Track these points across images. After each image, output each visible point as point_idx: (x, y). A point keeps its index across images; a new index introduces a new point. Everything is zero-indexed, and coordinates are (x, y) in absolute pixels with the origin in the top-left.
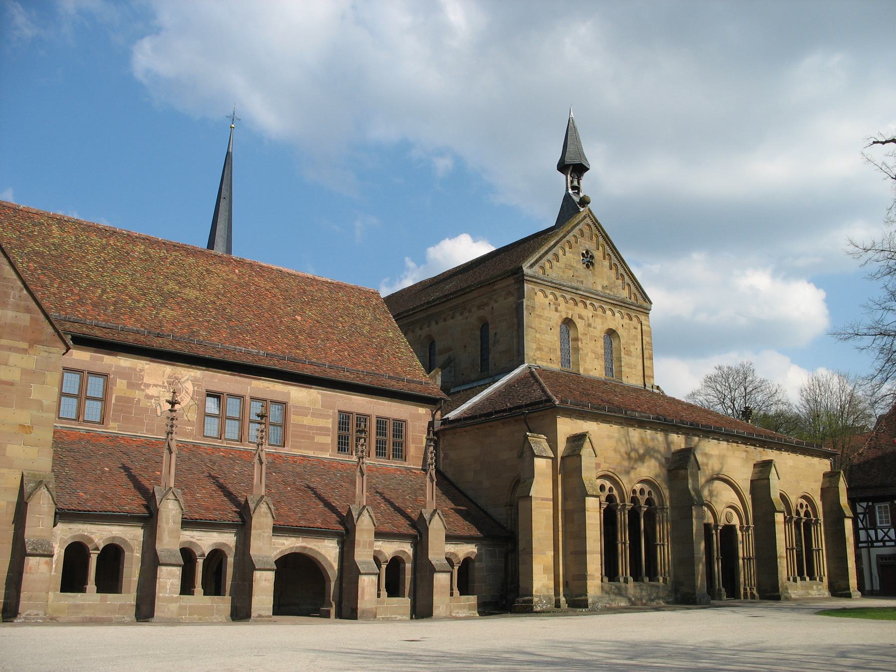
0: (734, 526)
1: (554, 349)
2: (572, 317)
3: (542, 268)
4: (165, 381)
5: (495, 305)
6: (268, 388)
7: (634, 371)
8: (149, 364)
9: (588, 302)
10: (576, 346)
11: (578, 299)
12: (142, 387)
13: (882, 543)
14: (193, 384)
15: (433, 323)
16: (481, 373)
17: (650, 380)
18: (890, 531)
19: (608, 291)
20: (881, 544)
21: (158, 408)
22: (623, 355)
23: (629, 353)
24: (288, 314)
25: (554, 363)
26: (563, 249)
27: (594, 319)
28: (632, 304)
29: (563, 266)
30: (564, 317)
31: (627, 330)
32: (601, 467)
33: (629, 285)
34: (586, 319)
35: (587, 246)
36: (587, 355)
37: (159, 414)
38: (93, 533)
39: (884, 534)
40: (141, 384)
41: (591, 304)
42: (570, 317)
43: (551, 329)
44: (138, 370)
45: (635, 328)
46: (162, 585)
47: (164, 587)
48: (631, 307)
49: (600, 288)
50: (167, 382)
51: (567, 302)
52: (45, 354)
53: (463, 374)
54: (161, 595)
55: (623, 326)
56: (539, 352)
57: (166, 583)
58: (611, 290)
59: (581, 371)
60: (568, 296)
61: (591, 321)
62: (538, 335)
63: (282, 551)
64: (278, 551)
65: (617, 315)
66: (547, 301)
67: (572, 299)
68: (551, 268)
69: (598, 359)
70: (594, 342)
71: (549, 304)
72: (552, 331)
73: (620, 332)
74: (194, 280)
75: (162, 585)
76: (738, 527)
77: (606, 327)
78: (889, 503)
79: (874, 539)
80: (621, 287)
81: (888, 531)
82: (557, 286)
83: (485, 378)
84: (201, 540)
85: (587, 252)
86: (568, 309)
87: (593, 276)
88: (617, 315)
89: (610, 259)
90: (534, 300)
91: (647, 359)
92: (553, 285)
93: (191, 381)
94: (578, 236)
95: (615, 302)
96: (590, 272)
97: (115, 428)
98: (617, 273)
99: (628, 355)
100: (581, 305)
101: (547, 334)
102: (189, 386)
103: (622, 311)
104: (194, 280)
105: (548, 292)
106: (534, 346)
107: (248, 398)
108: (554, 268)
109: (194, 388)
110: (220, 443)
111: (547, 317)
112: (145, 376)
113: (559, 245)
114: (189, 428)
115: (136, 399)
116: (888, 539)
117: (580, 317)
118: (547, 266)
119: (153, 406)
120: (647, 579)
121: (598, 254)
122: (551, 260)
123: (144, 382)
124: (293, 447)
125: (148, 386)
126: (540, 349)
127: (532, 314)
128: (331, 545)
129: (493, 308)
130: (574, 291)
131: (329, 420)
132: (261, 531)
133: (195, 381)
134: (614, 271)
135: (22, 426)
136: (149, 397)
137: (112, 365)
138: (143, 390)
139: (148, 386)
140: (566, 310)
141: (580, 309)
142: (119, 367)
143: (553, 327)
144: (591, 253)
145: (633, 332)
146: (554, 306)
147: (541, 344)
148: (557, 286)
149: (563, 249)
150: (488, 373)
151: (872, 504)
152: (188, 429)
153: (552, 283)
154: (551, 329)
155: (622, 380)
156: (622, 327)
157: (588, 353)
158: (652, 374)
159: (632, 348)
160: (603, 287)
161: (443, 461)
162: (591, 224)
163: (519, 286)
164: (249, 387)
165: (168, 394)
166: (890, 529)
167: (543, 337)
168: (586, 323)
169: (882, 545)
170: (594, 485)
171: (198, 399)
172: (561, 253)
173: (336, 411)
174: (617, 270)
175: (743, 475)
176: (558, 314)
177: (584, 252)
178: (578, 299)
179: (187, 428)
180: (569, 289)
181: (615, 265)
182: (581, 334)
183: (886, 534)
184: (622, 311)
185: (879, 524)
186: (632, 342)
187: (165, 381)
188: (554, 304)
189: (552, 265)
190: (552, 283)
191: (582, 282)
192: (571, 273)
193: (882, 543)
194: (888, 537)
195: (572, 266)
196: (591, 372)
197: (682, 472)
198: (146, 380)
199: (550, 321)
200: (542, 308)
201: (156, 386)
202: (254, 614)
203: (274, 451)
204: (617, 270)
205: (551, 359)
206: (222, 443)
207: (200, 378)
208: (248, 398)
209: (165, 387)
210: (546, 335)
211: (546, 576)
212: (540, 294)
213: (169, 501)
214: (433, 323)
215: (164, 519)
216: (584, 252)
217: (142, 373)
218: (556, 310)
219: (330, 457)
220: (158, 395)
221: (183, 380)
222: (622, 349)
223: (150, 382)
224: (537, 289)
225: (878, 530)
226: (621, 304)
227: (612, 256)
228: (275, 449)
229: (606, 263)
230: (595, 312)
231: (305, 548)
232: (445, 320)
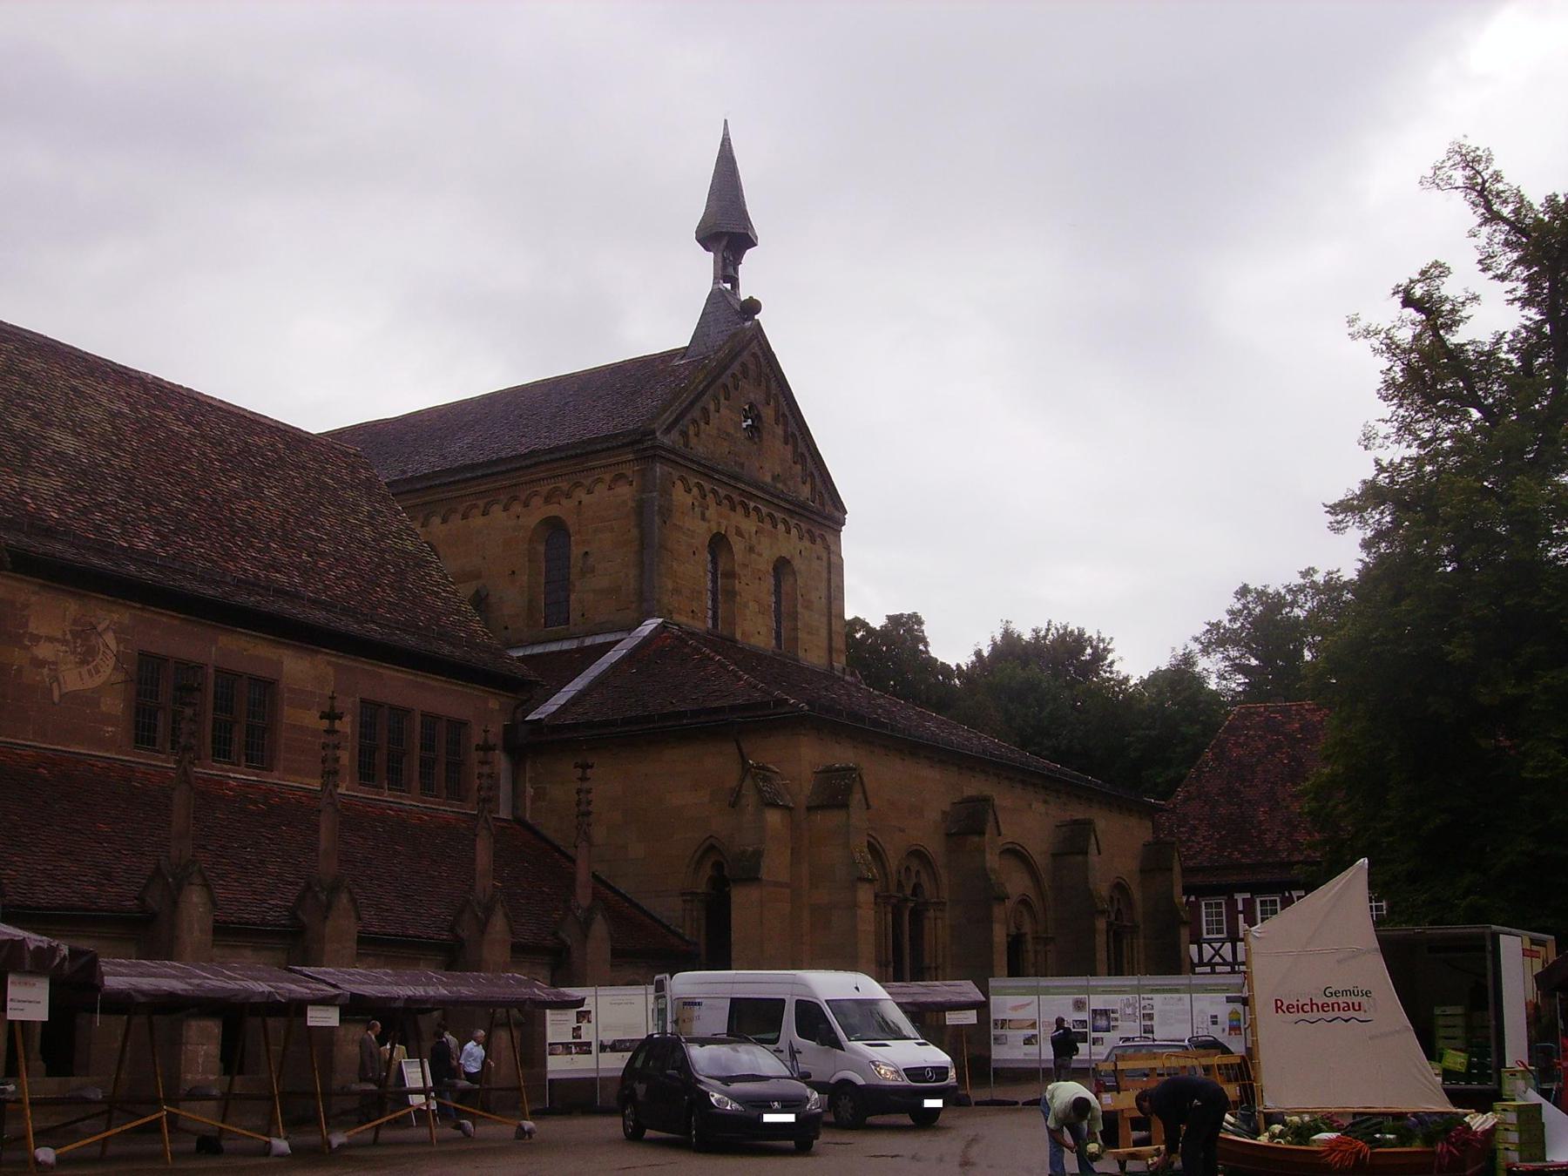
0: (1026, 934)
2: (726, 532)
3: (684, 434)
5: (586, 498)
6: (245, 650)
9: (752, 505)
11: (737, 498)
13: (1229, 967)
14: (116, 638)
15: (437, 520)
16: (545, 627)
18: (1224, 947)
19: (780, 486)
20: (1208, 969)
21: (55, 684)
22: (800, 609)
23: (808, 605)
25: (698, 619)
26: (716, 398)
34: (747, 536)
35: (752, 396)
37: (56, 699)
39: (1213, 952)
41: (756, 509)
43: (694, 553)
45: (818, 558)
48: (815, 517)
49: (768, 479)
51: (719, 504)
53: (506, 628)
59: (738, 636)
60: (722, 492)
65: (794, 531)
66: (689, 500)
67: (728, 497)
68: (697, 435)
70: (757, 581)
71: (693, 504)
73: (797, 563)
74: (59, 411)
76: (1029, 937)
78: (1226, 898)
79: (1196, 960)
81: (1221, 947)
82: (707, 470)
83: (562, 639)
85: (751, 406)
88: (794, 531)
89: (786, 424)
90: (671, 495)
92: (701, 469)
93: (115, 632)
94: (740, 376)
95: (791, 507)
96: (755, 446)
100: (739, 509)
104: (59, 411)
105: (693, 480)
106: (670, 585)
108: (703, 435)
114: (110, 729)
115: (15, 667)
116: (1221, 961)
117: (739, 533)
118: (691, 432)
119: (45, 682)
121: (768, 413)
122: (698, 419)
123: (30, 630)
125: (36, 639)
127: (668, 522)
129: (580, 502)
134: (789, 447)
136: (39, 663)
139: (36, 639)
140: (719, 518)
141: (738, 518)
144: (759, 411)
146: (700, 509)
147: (678, 581)
148: (707, 470)
149: (716, 398)
150: (568, 629)
151: (1196, 899)
152: (108, 732)
153: (699, 464)
154: (694, 553)
161: (533, 802)
162: (760, 354)
163: (643, 467)
165: (72, 658)
166: (1224, 943)
169: (1230, 970)
172: (712, 407)
173: (358, 700)
175: (1040, 845)
176: (705, 525)
177: (747, 407)
178: (737, 498)
179: (105, 728)
180: (725, 479)
181: (793, 435)
182: (739, 565)
183: (1217, 952)
184: (802, 525)
185: (1205, 936)
188: (700, 506)
189: (698, 430)
190: (699, 464)
191: (742, 465)
193: (1229, 967)
194: (1221, 956)
195: (728, 434)
197: (976, 839)
198: (33, 627)
200: (683, 513)
201: (50, 639)
203: (255, 778)
204: (795, 446)
205: (693, 611)
212: (679, 483)
213: (193, 887)
214: (437, 520)
216: (747, 407)
218: (703, 518)
219: (347, 793)
220: (54, 659)
222: (799, 597)
223: (43, 631)
224: (676, 474)
225: (1204, 945)
226: (801, 511)
228: (257, 776)
229: (779, 431)
230: (760, 524)
232: (465, 517)
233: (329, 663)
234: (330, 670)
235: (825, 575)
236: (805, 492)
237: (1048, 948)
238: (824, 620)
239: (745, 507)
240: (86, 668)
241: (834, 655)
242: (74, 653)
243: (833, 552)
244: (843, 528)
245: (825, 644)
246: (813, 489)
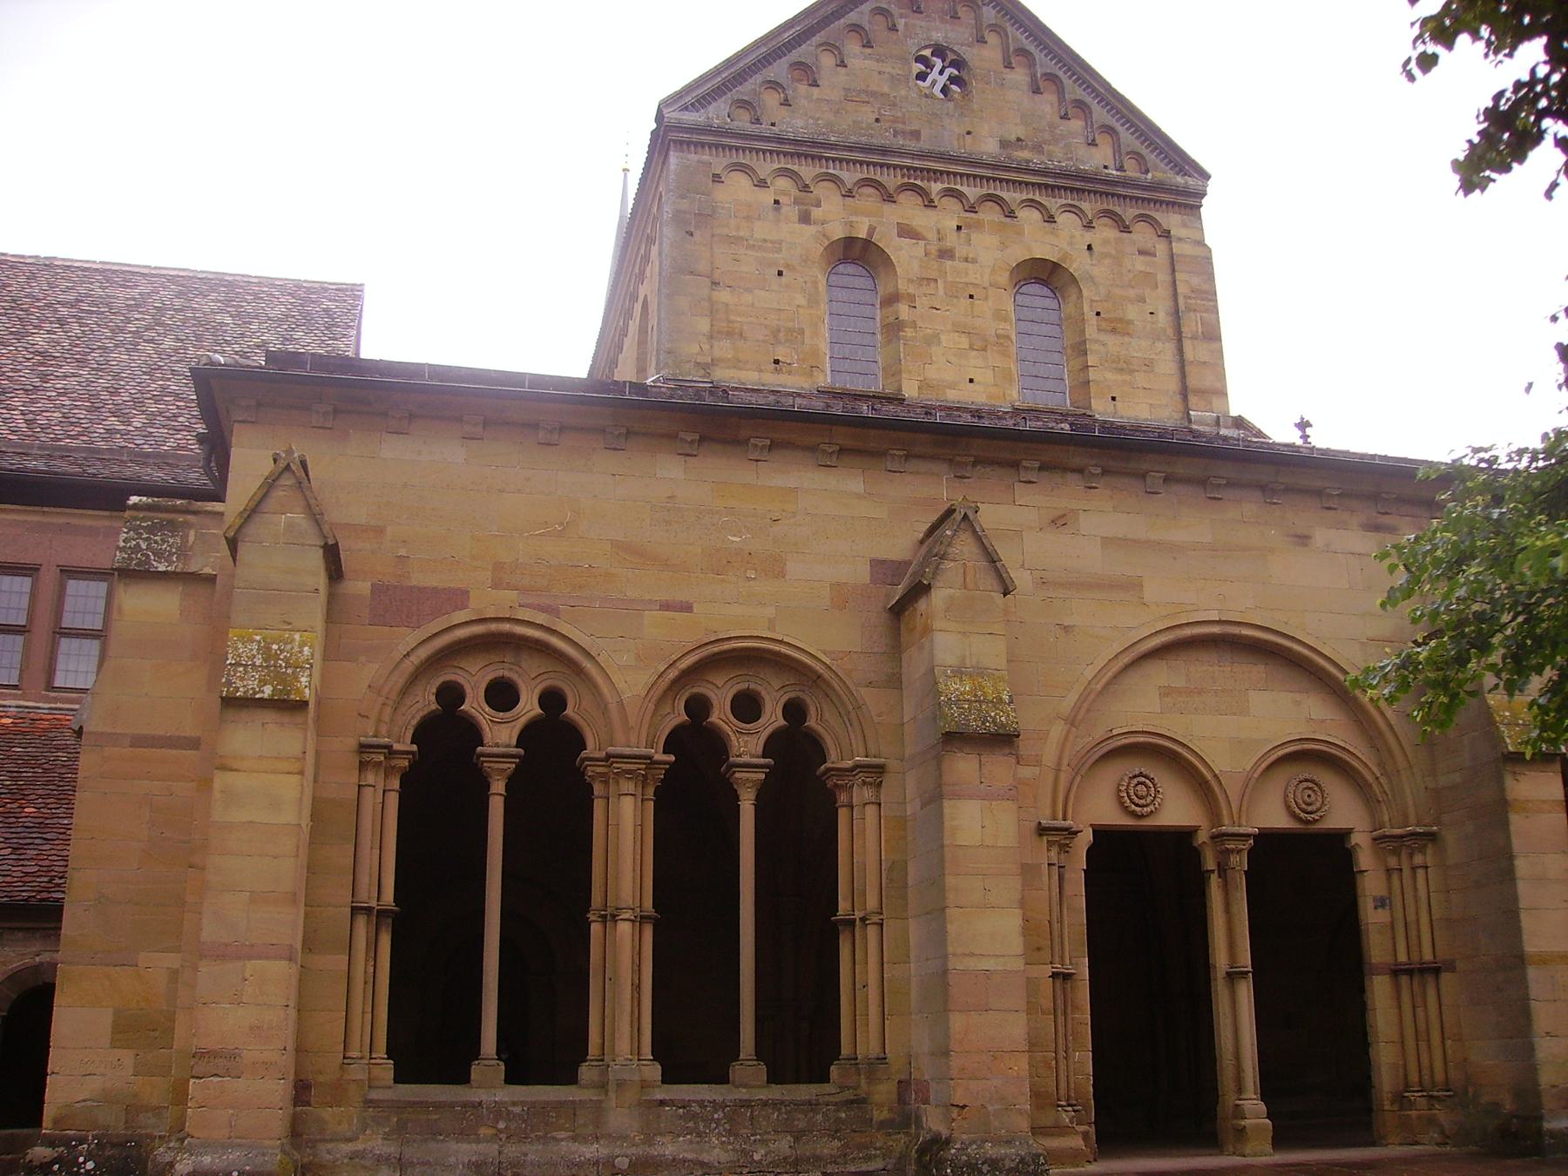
0: (1342, 836)
1: (790, 331)
7: (1141, 379)
10: (891, 319)
17: (1211, 403)
19: (1025, 154)
22: (1091, 331)
23: (1118, 327)
25: (790, 373)
27: (968, 234)
28: (1126, 183)
29: (836, 95)
30: (838, 232)
31: (1107, 261)
32: (473, 603)
33: (1109, 130)
34: (932, 236)
35: (938, 36)
36: (933, 339)
41: (950, 193)
42: (863, 235)
43: (780, 273)
55: (1089, 248)
56: (727, 344)
58: (1038, 148)
59: (910, 391)
60: (849, 176)
61: (952, 240)
62: (724, 296)
65: (1064, 219)
66: (767, 197)
69: (984, 349)
71: (776, 202)
72: (783, 279)
73: (1079, 264)
77: (1018, 254)
80: (1081, 140)
86: (856, 212)
87: (962, 114)
91: (1194, 338)
92: (788, 148)
98: (1061, 99)
99: (1114, 331)
100: (909, 202)
101: (763, 289)
103: (1085, 206)
105: (765, 167)
106: (704, 325)
111: (765, 241)
113: (817, 39)
117: (906, 232)
120: (748, 1070)
121: (983, 58)
126: (730, 334)
130: (876, 159)
141: (909, 210)
143: (787, 266)
145: (1140, 264)
154: (780, 273)
155: (1090, 407)
156: (1087, 253)
157: (937, 336)
158: (1218, 385)
159: (1132, 312)
160: (1004, 144)
167: (748, 298)
168: (933, 249)
170: (286, 660)
174: (1061, 91)
176: (810, 230)
184: (1085, 206)
186: (1132, 293)
188: (796, 202)
192: (867, 115)
195: (874, 94)
196: (948, 391)
199: (779, 251)
205: (777, 362)
210: (762, 293)
218: (805, 218)
222: (1089, 315)
224: (719, 162)
227: (1039, 56)
229: (1019, 76)
235: (1163, 277)
236: (1097, 159)
237: (1418, 859)
238: (1169, 348)
239: (922, 192)
241: (1193, 400)
243: (1180, 239)
244: (1204, 201)
245: (1173, 385)
246: (1117, 149)
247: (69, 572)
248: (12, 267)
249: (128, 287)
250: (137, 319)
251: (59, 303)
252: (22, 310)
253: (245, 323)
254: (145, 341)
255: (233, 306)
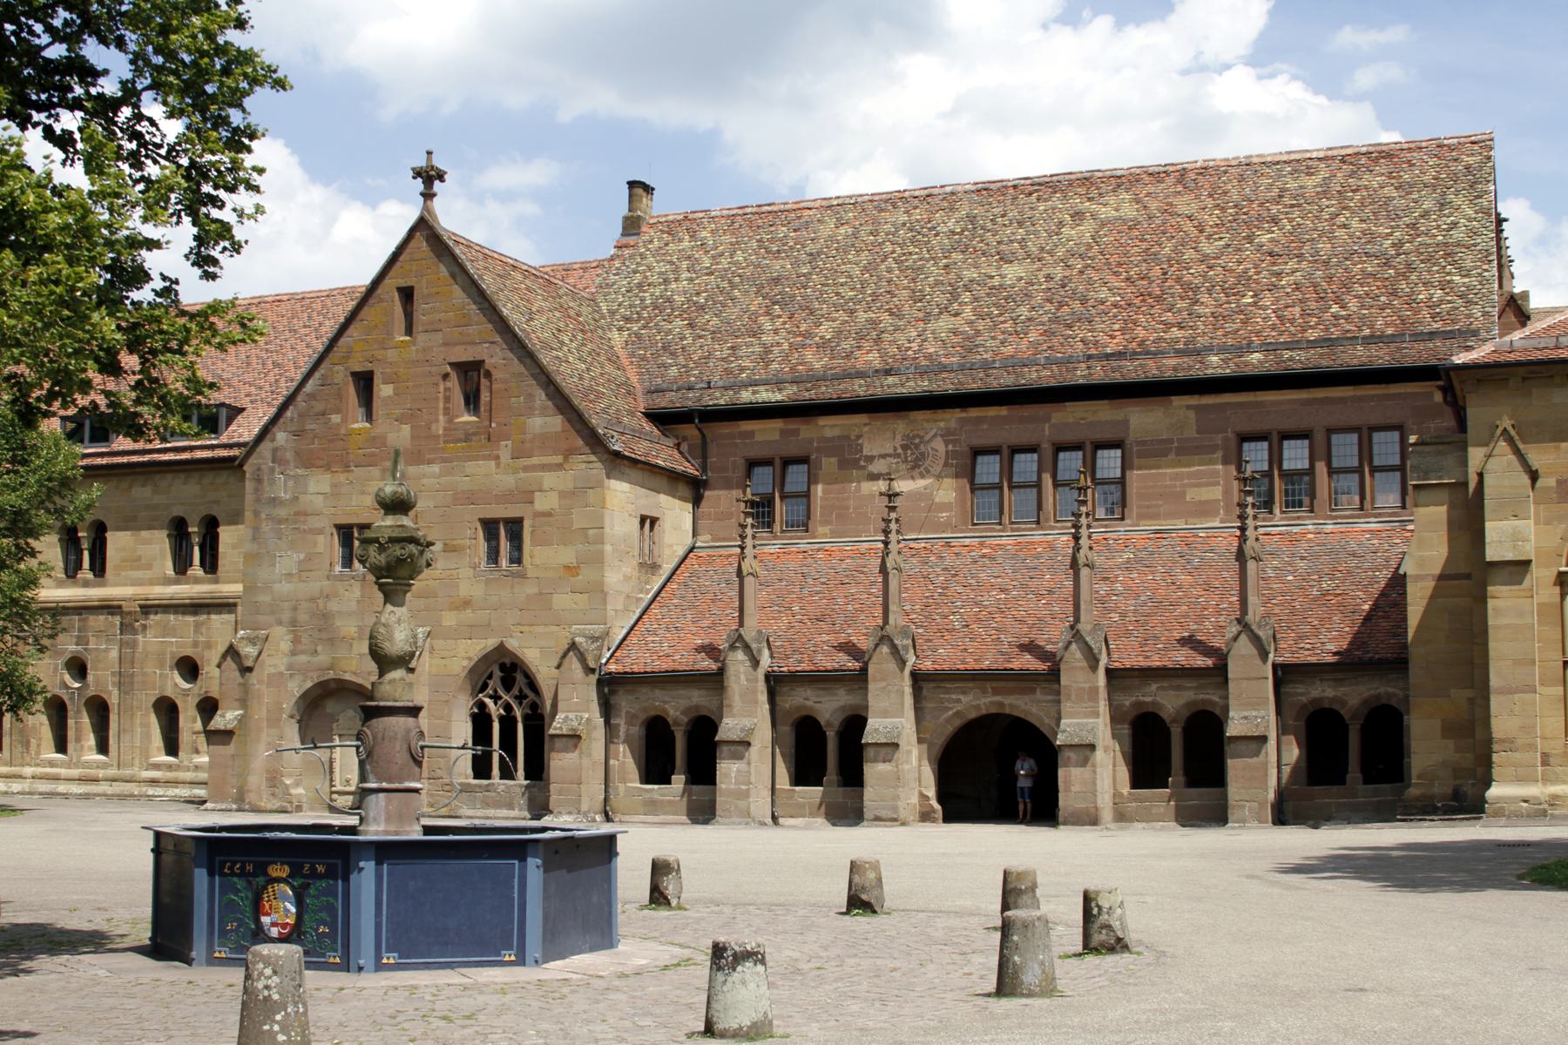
4: (898, 445)
8: (869, 424)
12: (862, 463)
14: (944, 441)
24: (1204, 259)
38: (666, 702)
40: (860, 459)
44: (853, 438)
46: (724, 771)
47: (727, 775)
50: (902, 446)
52: (583, 466)
54: (724, 786)
57: (730, 769)
63: (958, 714)
64: (950, 713)
75: (724, 771)
84: (820, 702)
93: (942, 436)
97: (825, 536)
102: (939, 445)
107: (1046, 446)
109: (947, 446)
110: (999, 531)
112: (865, 445)
123: (865, 453)
124: (1141, 517)
125: (870, 459)
128: (1049, 698)
131: (1215, 456)
132: (883, 684)
133: (947, 435)
135: (567, 568)
137: (813, 439)
138: (864, 468)
139: (870, 459)
142: (823, 439)
164: (1047, 425)
171: (957, 463)
187: (898, 445)
198: (866, 452)
201: (884, 456)
202: (868, 814)
206: (1003, 531)
207: (956, 429)
208: (1046, 446)
209: (898, 456)
211: (1450, 743)
215: (733, 678)
217: (860, 442)
221: (927, 438)
231: (1001, 704)
233: (1189, 407)
234: (1192, 414)
240: (917, 471)
242: (906, 461)
247: (1330, 431)
248: (1226, 172)
249: (1312, 174)
250: (1327, 207)
251: (1268, 201)
252: (1245, 214)
253: (1408, 193)
254: (1339, 227)
255: (1394, 177)
